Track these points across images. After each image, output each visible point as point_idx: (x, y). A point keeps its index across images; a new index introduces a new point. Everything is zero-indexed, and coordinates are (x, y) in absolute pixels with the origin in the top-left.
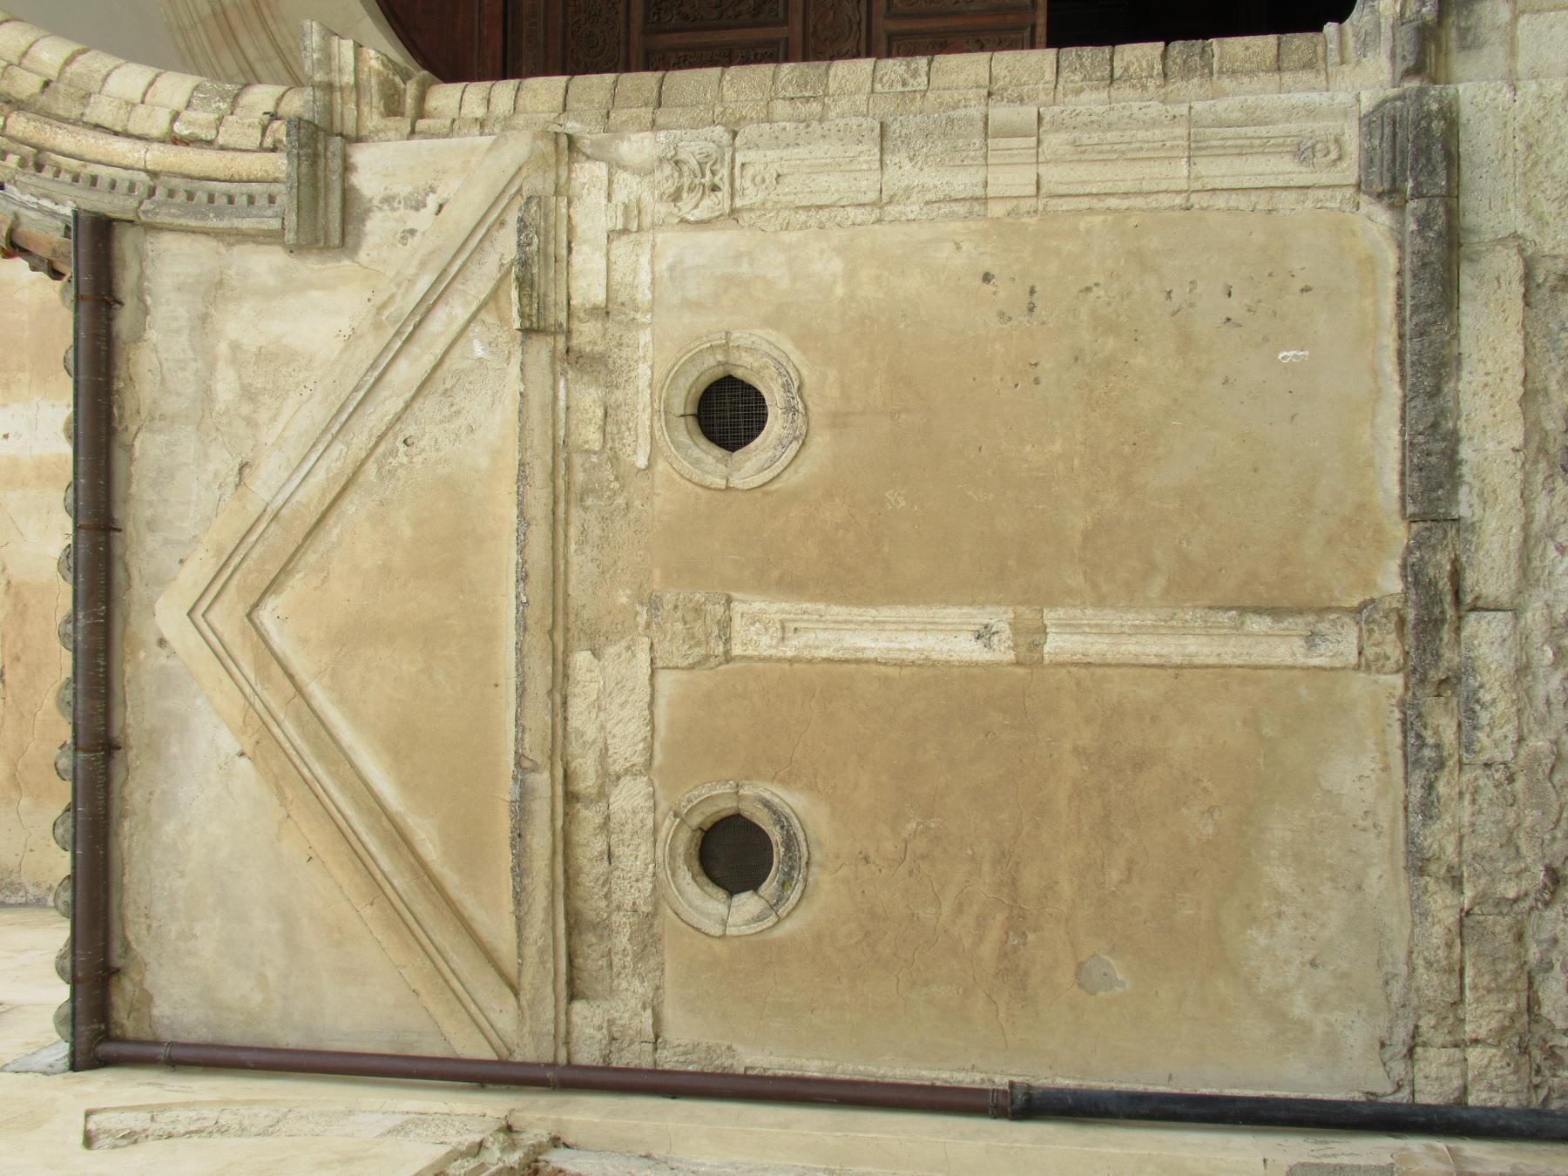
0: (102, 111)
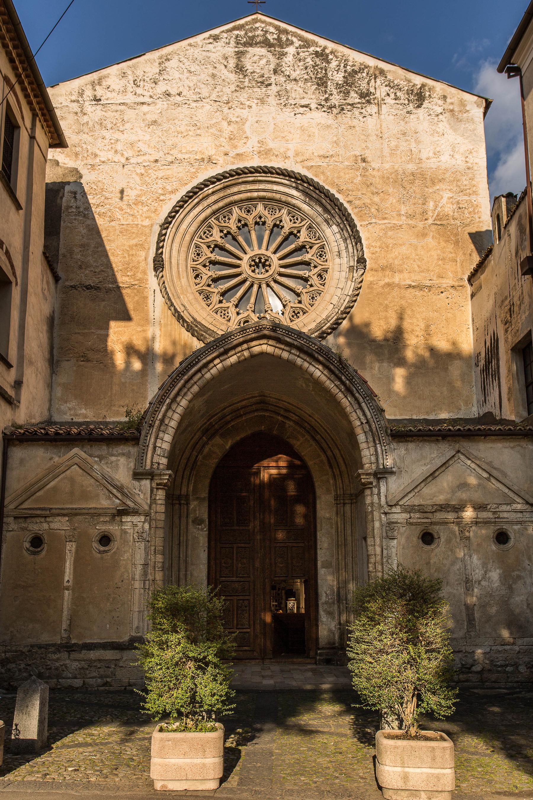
0: (161, 435)
